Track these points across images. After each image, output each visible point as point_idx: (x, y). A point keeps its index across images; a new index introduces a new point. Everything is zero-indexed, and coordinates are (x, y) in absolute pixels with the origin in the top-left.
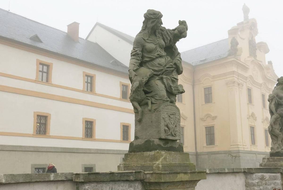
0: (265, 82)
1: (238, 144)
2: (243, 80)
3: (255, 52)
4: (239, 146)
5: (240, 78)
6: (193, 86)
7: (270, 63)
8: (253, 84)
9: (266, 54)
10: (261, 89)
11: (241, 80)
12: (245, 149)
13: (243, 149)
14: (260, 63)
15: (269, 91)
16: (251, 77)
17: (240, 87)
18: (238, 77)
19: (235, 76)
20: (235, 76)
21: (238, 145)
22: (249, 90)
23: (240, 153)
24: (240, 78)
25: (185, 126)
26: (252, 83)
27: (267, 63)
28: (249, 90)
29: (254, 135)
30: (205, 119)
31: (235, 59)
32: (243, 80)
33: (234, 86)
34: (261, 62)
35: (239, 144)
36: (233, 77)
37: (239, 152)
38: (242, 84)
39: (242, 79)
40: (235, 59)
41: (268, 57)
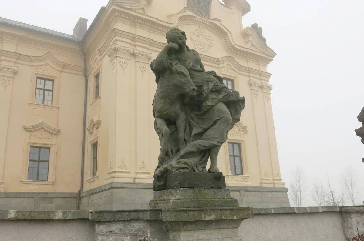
0: (231, 56)
1: (114, 170)
4: (117, 174)
5: (137, 43)
6: (86, 77)
12: (137, 181)
13: (131, 181)
15: (249, 73)
17: (137, 60)
19: (118, 38)
20: (118, 38)
21: (115, 172)
23: (113, 190)
24: (137, 43)
25: (52, 145)
30: (91, 131)
31: (115, 7)
33: (117, 57)
34: (220, 21)
35: (116, 170)
36: (116, 40)
37: (111, 188)
40: (115, 7)
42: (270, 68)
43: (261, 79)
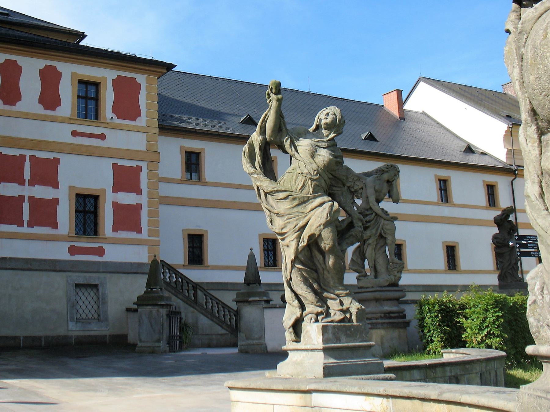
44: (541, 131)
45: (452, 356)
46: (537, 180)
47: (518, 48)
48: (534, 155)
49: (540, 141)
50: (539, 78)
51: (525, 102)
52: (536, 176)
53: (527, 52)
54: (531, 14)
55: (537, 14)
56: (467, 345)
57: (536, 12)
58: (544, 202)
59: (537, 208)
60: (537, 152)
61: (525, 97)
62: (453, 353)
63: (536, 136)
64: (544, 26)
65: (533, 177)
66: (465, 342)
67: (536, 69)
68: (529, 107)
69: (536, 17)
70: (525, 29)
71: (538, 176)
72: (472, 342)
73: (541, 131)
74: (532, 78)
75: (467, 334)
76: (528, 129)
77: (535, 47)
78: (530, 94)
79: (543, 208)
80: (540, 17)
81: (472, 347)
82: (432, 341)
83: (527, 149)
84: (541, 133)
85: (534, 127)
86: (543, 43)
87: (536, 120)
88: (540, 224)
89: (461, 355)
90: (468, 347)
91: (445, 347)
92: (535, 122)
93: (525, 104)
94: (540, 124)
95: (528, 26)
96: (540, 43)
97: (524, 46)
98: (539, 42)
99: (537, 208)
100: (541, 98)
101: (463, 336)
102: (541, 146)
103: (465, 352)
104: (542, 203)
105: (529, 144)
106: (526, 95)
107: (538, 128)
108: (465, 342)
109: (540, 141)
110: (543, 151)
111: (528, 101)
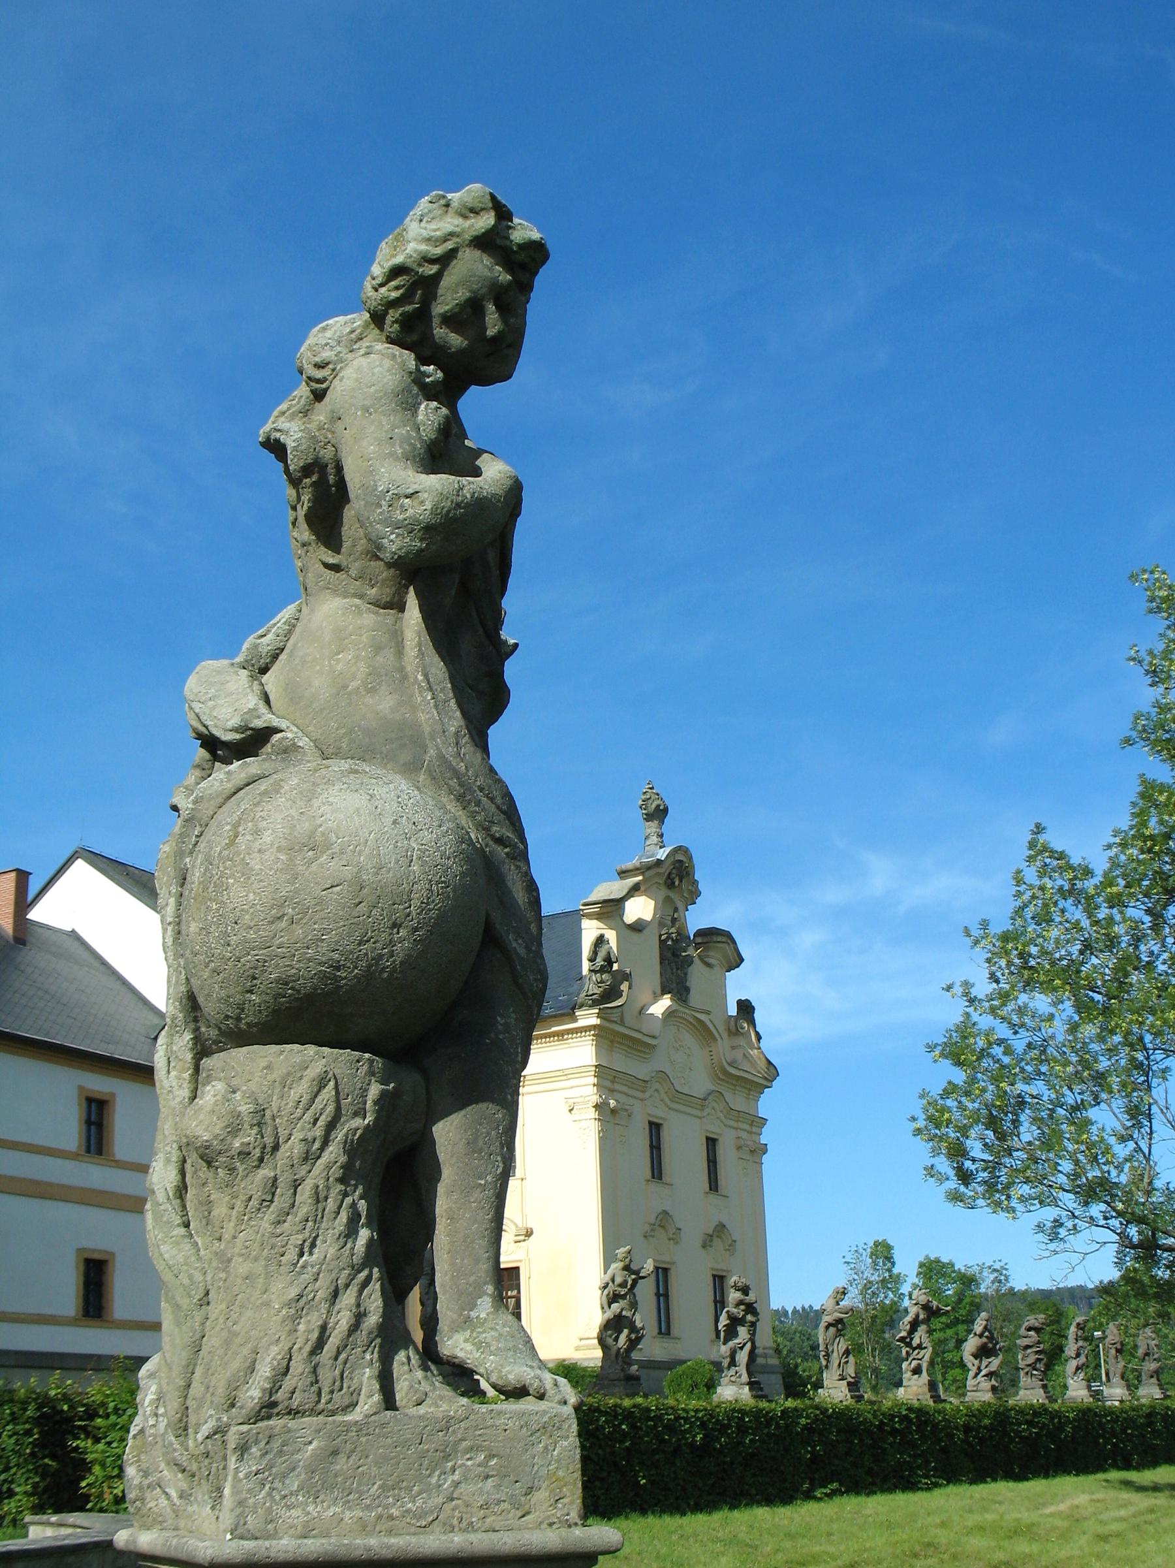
2: (630, 1092)
3: (686, 974)
5: (618, 1087)
7: (746, 1008)
8: (669, 1102)
9: (728, 971)
10: (700, 1118)
11: (626, 1094)
14: (702, 1017)
16: (662, 1076)
18: (613, 1082)
22: (655, 1128)
24: (618, 1087)
26: (667, 1100)
27: (733, 1010)
28: (655, 1128)
29: (666, 1296)
32: (630, 1092)
34: (708, 1013)
38: (627, 1110)
39: (625, 1089)
41: (738, 986)
42: (767, 1104)
43: (750, 1133)
44: (203, 1045)
45: (49, 1532)
46: (175, 1156)
47: (179, 854)
48: (178, 1100)
49: (197, 1069)
50: (205, 930)
51: (177, 977)
52: (175, 1146)
53: (193, 866)
54: (217, 784)
55: (230, 786)
56: (89, 1506)
57: (229, 781)
58: (184, 1207)
59: (165, 1219)
60: (186, 1093)
61: (179, 965)
62: (52, 1524)
63: (189, 1056)
64: (235, 817)
65: (168, 1149)
66: (86, 1498)
67: (203, 907)
68: (183, 989)
69: (227, 793)
70: (198, 815)
71: (180, 1148)
72: (100, 1496)
73: (203, 1045)
74: (194, 927)
75: (91, 1479)
76: (176, 1038)
77: (208, 860)
78: (187, 963)
79: (178, 1220)
80: (235, 793)
81: (101, 1510)
82: (11, 1494)
83: (166, 1084)
84: (202, 1050)
85: (188, 1036)
86: (226, 853)
87: (196, 1020)
88: (166, 1256)
89: (69, 1531)
90: (90, 1510)
91: (39, 1509)
92: (192, 1025)
93: (177, 982)
94: (203, 1029)
95: (206, 809)
96: (221, 852)
97: (191, 853)
98: (218, 849)
99: (165, 1219)
100: (206, 975)
101: (83, 1484)
102: (197, 1081)
103: (78, 1522)
104: (179, 1209)
105: (173, 1073)
106: (182, 962)
107: (197, 1039)
108: (86, 1498)
109: (197, 1069)
110: (199, 1093)
111: (183, 977)
